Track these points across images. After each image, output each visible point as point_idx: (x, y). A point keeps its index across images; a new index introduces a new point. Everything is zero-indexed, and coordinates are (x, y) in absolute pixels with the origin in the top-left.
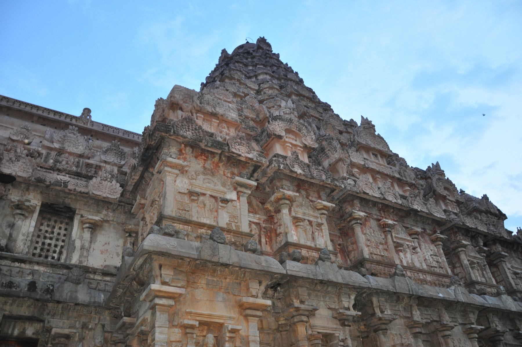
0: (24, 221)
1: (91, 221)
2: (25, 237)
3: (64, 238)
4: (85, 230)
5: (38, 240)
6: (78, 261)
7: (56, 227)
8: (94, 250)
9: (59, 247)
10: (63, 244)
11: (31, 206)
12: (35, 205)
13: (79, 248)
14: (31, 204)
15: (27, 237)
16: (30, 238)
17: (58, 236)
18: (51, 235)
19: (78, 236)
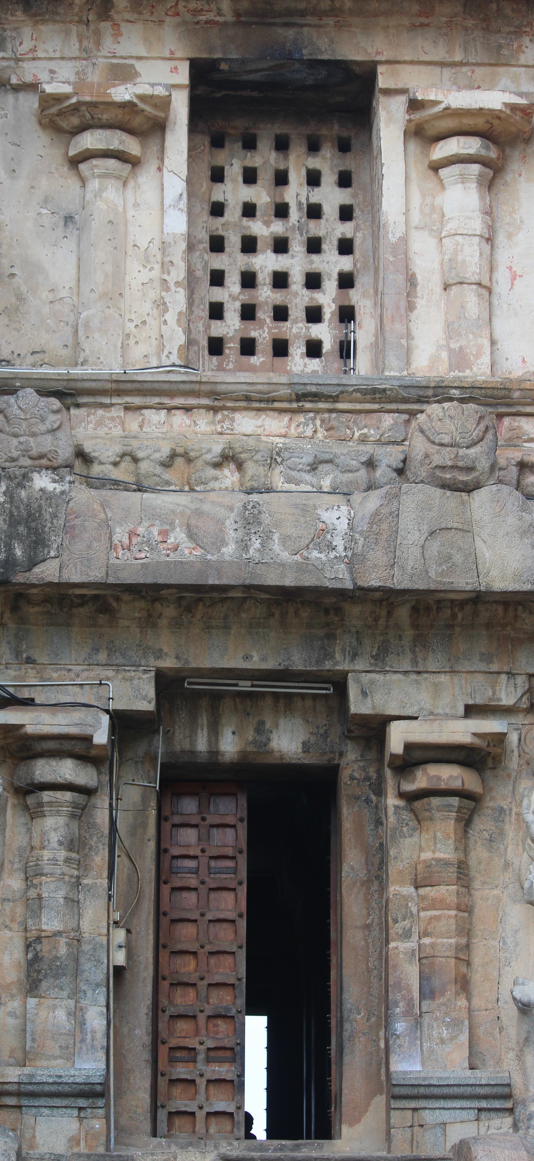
0: (131, 184)
1: (468, 122)
2: (156, 273)
3: (346, 229)
4: (443, 172)
5: (218, 262)
6: (444, 355)
7: (292, 177)
8: (514, 278)
9: (330, 285)
10: (346, 263)
11: (142, 98)
12: (160, 91)
13: (436, 282)
14: (143, 89)
15: (166, 266)
16: (179, 273)
17: (312, 224)
18: (278, 227)
19: (416, 217)
